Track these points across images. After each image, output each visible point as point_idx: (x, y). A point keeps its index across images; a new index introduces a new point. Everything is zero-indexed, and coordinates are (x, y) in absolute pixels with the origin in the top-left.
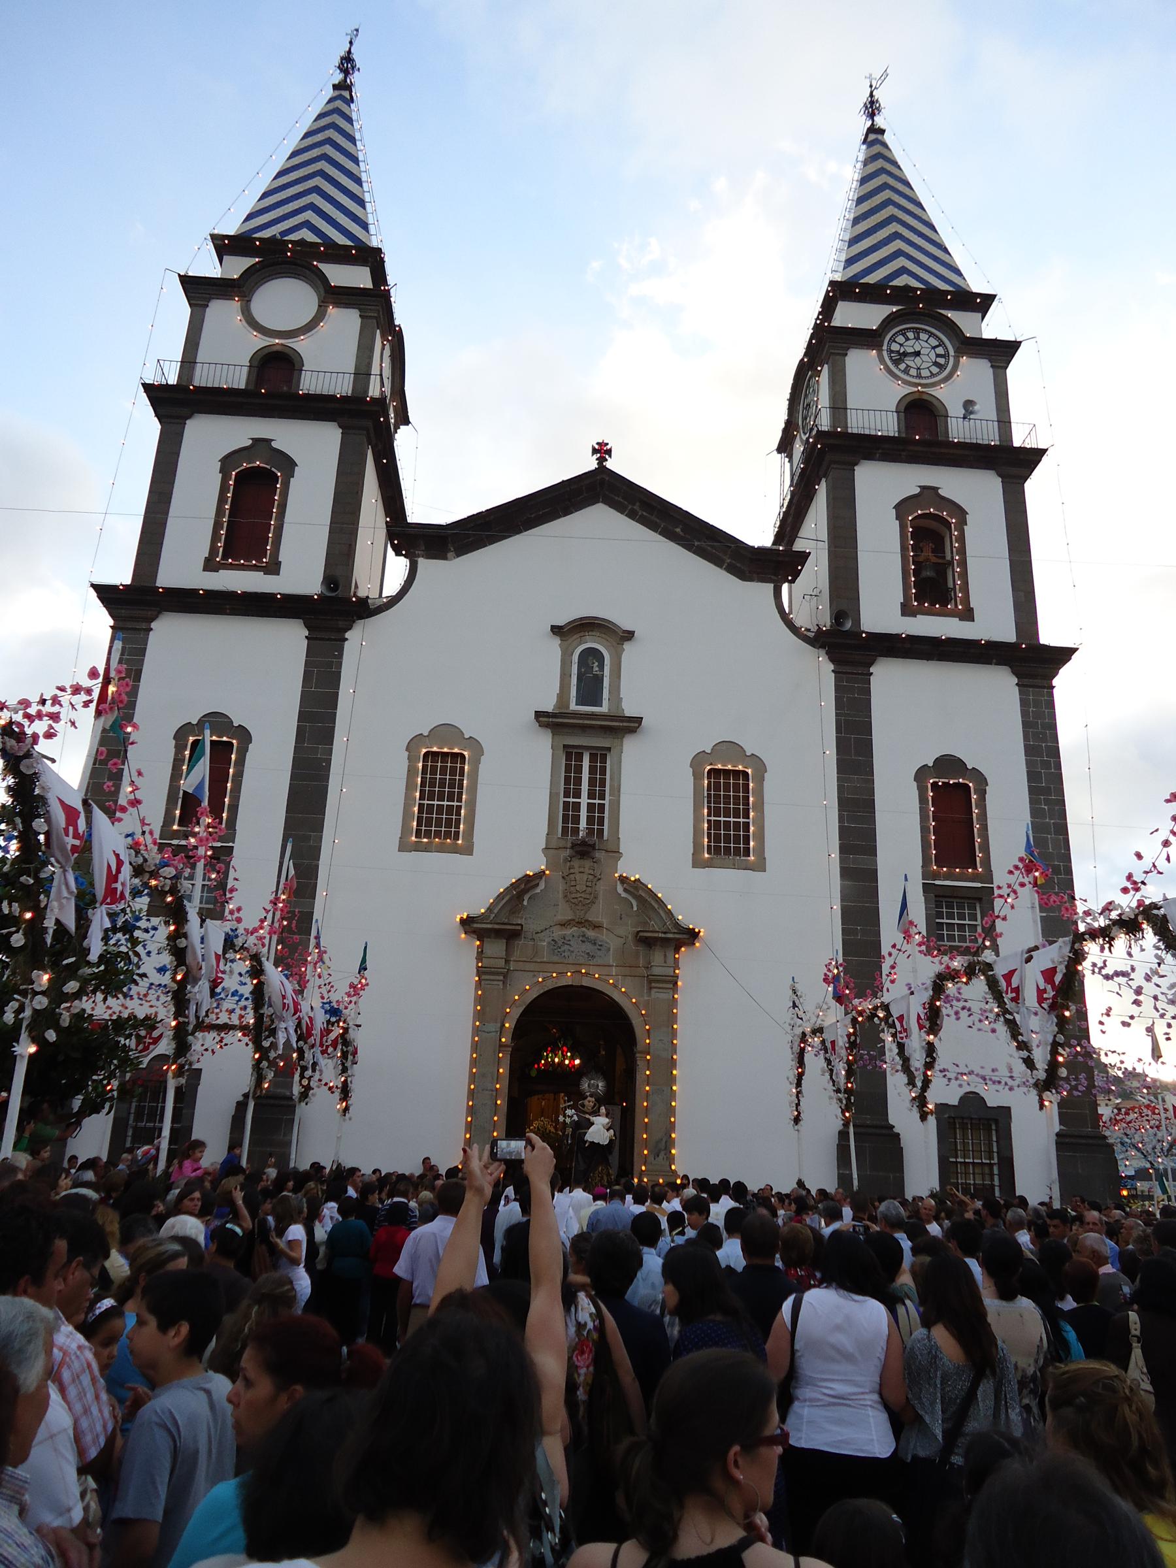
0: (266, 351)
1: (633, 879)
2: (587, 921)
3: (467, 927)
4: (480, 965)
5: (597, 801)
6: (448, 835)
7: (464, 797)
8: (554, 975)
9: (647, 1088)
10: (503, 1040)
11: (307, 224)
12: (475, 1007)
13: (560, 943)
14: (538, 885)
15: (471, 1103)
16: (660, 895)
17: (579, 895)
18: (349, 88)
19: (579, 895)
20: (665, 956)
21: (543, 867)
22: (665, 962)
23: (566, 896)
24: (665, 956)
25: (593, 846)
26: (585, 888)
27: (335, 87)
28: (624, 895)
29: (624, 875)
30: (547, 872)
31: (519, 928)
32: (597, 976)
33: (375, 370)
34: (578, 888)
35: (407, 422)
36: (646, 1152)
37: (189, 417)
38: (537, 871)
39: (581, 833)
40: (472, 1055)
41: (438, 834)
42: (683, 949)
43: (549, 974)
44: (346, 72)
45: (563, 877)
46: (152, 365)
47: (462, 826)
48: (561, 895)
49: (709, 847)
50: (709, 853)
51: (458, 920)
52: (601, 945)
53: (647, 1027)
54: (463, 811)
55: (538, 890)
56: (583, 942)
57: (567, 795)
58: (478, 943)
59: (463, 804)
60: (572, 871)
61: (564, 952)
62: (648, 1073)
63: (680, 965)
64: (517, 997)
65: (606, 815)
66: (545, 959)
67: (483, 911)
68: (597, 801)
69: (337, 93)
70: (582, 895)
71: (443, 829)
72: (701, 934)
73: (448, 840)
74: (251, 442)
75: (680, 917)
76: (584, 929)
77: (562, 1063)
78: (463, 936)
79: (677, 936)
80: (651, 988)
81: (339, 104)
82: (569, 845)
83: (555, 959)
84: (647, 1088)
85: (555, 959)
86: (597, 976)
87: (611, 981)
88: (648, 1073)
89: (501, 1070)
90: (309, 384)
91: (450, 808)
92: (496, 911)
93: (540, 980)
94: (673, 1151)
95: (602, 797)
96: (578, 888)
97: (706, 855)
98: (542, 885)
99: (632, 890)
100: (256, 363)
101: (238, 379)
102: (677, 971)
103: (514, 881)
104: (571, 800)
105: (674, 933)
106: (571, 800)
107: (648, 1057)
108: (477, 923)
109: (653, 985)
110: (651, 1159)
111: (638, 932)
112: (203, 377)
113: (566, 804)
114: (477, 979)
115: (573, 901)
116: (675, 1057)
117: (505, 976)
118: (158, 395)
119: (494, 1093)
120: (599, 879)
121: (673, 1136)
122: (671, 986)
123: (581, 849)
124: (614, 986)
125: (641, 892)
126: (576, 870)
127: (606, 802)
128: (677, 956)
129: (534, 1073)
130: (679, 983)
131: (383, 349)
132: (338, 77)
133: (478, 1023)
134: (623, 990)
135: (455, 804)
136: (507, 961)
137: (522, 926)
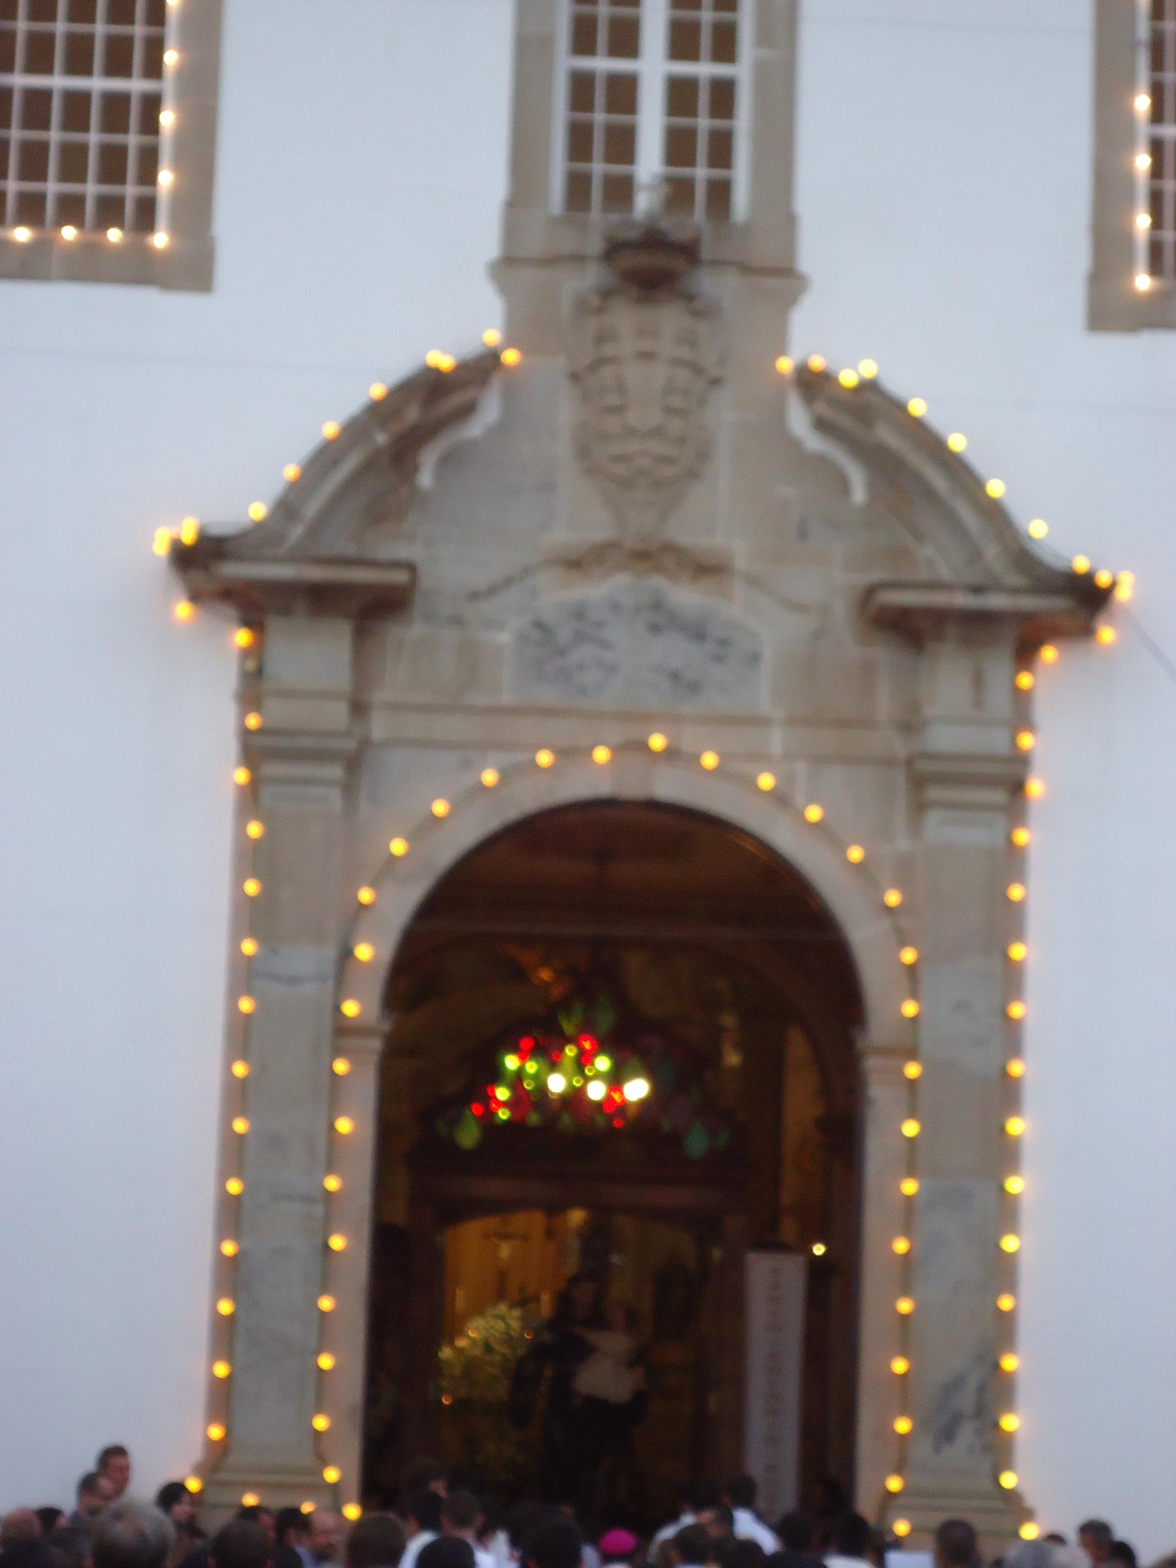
1: (848, 378)
2: (670, 548)
3: (198, 576)
4: (253, 721)
5: (704, 70)
6: (110, 211)
7: (171, 58)
8: (544, 758)
9: (909, 1187)
10: (351, 1008)
12: (238, 882)
13: (564, 635)
14: (468, 410)
15: (229, 1248)
16: (957, 443)
17: (633, 446)
19: (633, 446)
20: (978, 681)
21: (492, 337)
22: (978, 703)
23: (583, 452)
24: (978, 681)
25: (689, 252)
26: (655, 418)
28: (813, 442)
29: (817, 363)
30: (510, 357)
31: (400, 577)
32: (709, 760)
34: (633, 417)
36: (903, 1426)
38: (469, 349)
39: (644, 202)
40: (228, 1068)
41: (71, 209)
42: (1049, 654)
43: (520, 757)
45: (575, 377)
47: (166, 178)
48: (563, 449)
49: (1156, 250)
50: (1156, 268)
51: (161, 547)
52: (724, 642)
53: (908, 956)
54: (167, 119)
55: (475, 428)
56: (655, 629)
57: (583, 41)
58: (242, 637)
59: (168, 86)
60: (608, 350)
61: (581, 667)
62: (911, 1129)
63: (1041, 710)
64: (398, 847)
65: (743, 123)
66: (507, 698)
67: (258, 511)
68: (704, 70)
70: (653, 446)
71: (91, 189)
72: (1123, 594)
73: (114, 235)
75: (1037, 529)
76: (658, 582)
77: (575, 1099)
78: (183, 610)
79: (1028, 603)
80: (919, 808)
82: (595, 245)
83: (548, 695)
84: (909, 1187)
85: (548, 695)
86: (709, 760)
87: (766, 781)
88: (911, 1129)
89: (344, 1126)
91: (116, 105)
92: (311, 509)
93: (489, 777)
94: (1010, 1423)
95: (725, 48)
96: (633, 417)
97: (1143, 282)
98: (490, 410)
99: (845, 421)
102: (1026, 741)
103: (378, 391)
104: (602, 64)
105: (1015, 591)
106: (602, 64)
107: (913, 1070)
108: (239, 558)
109: (935, 793)
110: (923, 1450)
111: (870, 592)
113: (582, 86)
114: (241, 776)
115: (620, 469)
116: (1016, 1068)
117: (354, 763)
119: (319, 1210)
120: (716, 382)
121: (1009, 1363)
122: (998, 796)
123: (643, 260)
124: (780, 798)
125: (886, 435)
126: (626, 346)
127: (742, 71)
128: (1025, 680)
129: (469, 1136)
130: (1035, 787)
133: (249, 947)
134: (814, 813)
135: (136, 85)
136: (359, 708)
137: (411, 568)
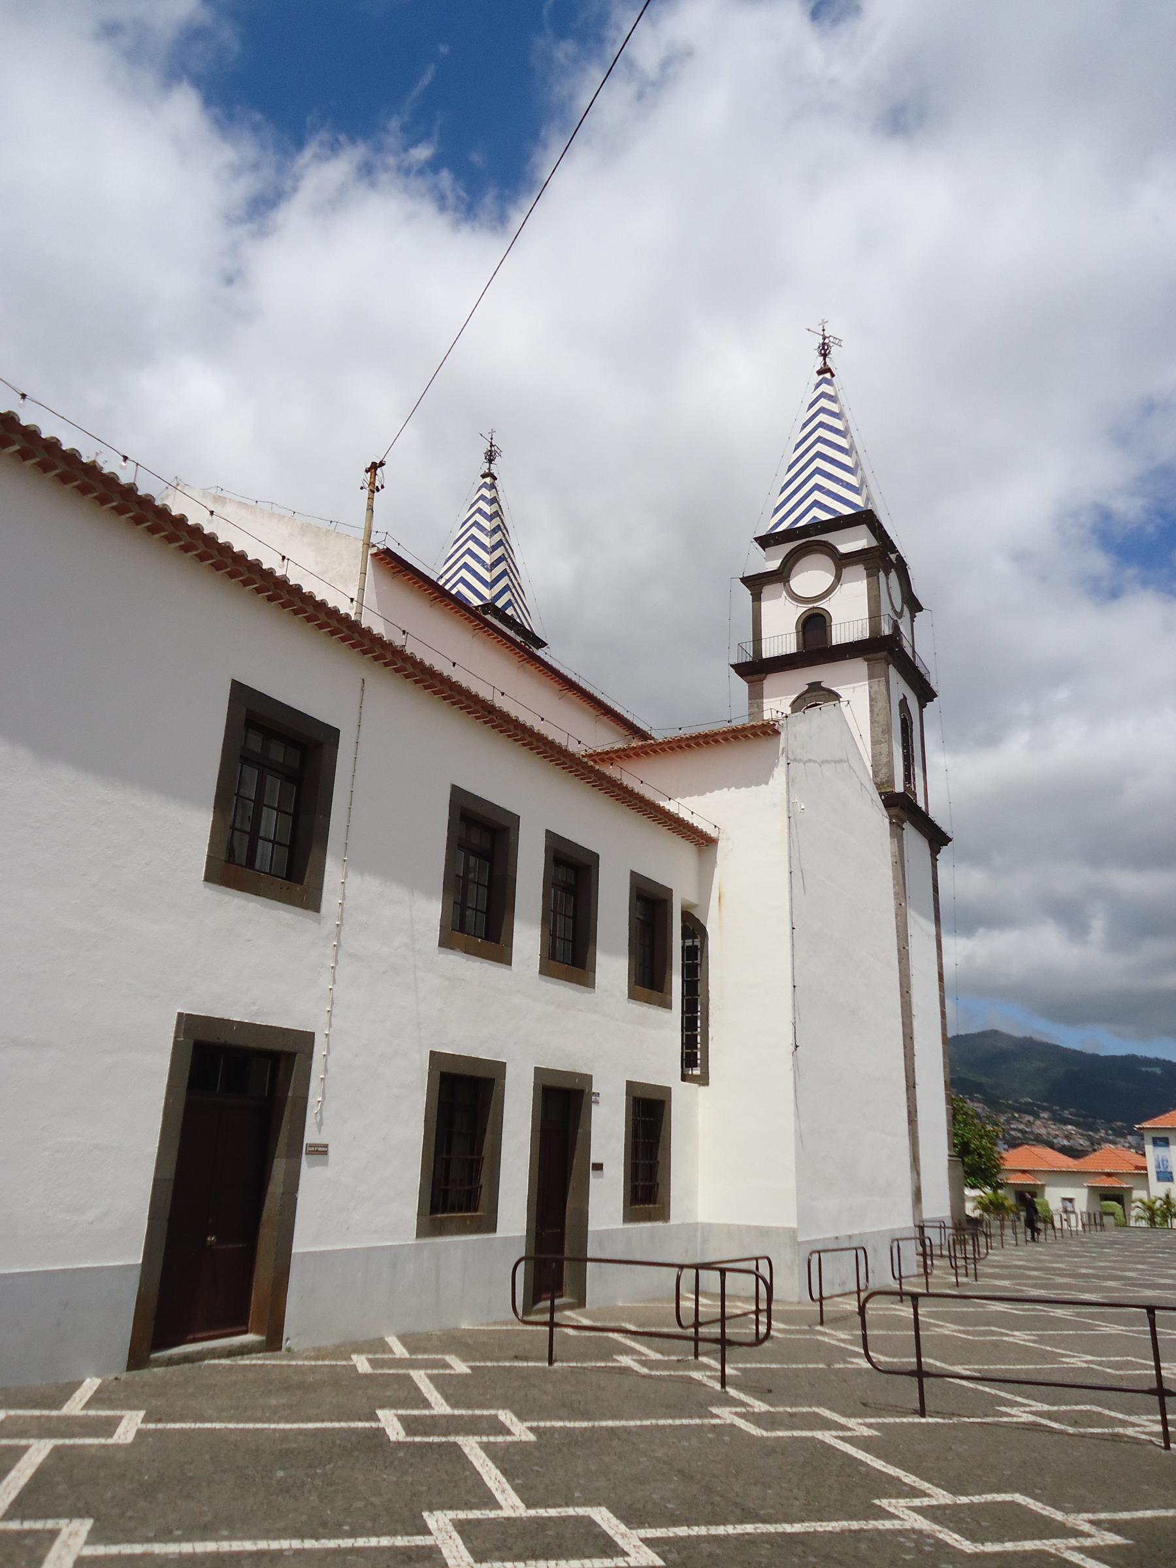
0: (804, 617)
11: (816, 503)
18: (829, 370)
27: (820, 373)
33: (886, 609)
35: (920, 609)
37: (764, 678)
44: (825, 356)
46: (735, 648)
69: (821, 376)
74: (807, 686)
81: (824, 388)
90: (840, 635)
100: (800, 629)
101: (789, 645)
112: (768, 651)
118: (742, 669)
131: (887, 578)
132: (819, 363)
